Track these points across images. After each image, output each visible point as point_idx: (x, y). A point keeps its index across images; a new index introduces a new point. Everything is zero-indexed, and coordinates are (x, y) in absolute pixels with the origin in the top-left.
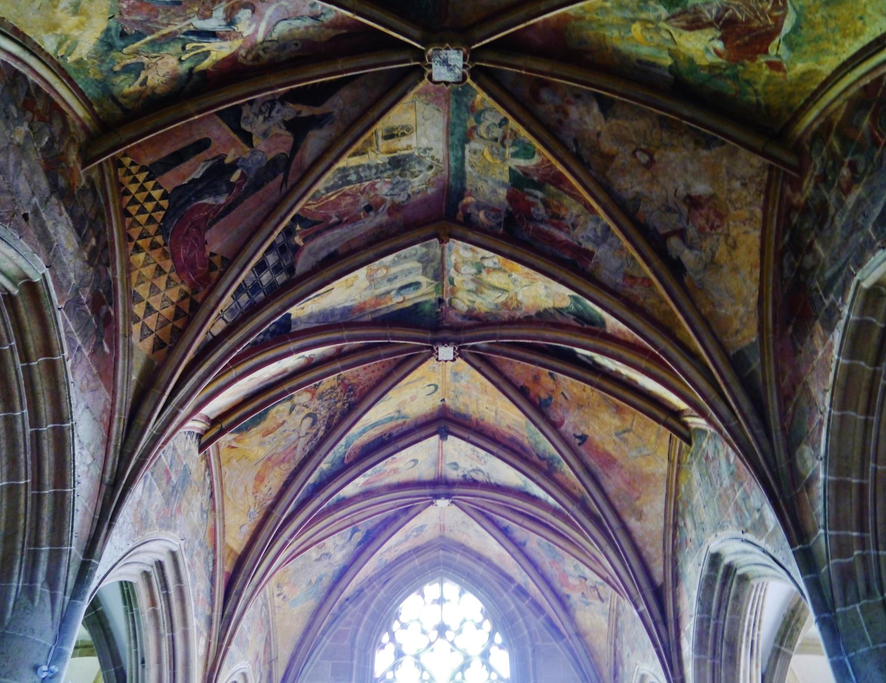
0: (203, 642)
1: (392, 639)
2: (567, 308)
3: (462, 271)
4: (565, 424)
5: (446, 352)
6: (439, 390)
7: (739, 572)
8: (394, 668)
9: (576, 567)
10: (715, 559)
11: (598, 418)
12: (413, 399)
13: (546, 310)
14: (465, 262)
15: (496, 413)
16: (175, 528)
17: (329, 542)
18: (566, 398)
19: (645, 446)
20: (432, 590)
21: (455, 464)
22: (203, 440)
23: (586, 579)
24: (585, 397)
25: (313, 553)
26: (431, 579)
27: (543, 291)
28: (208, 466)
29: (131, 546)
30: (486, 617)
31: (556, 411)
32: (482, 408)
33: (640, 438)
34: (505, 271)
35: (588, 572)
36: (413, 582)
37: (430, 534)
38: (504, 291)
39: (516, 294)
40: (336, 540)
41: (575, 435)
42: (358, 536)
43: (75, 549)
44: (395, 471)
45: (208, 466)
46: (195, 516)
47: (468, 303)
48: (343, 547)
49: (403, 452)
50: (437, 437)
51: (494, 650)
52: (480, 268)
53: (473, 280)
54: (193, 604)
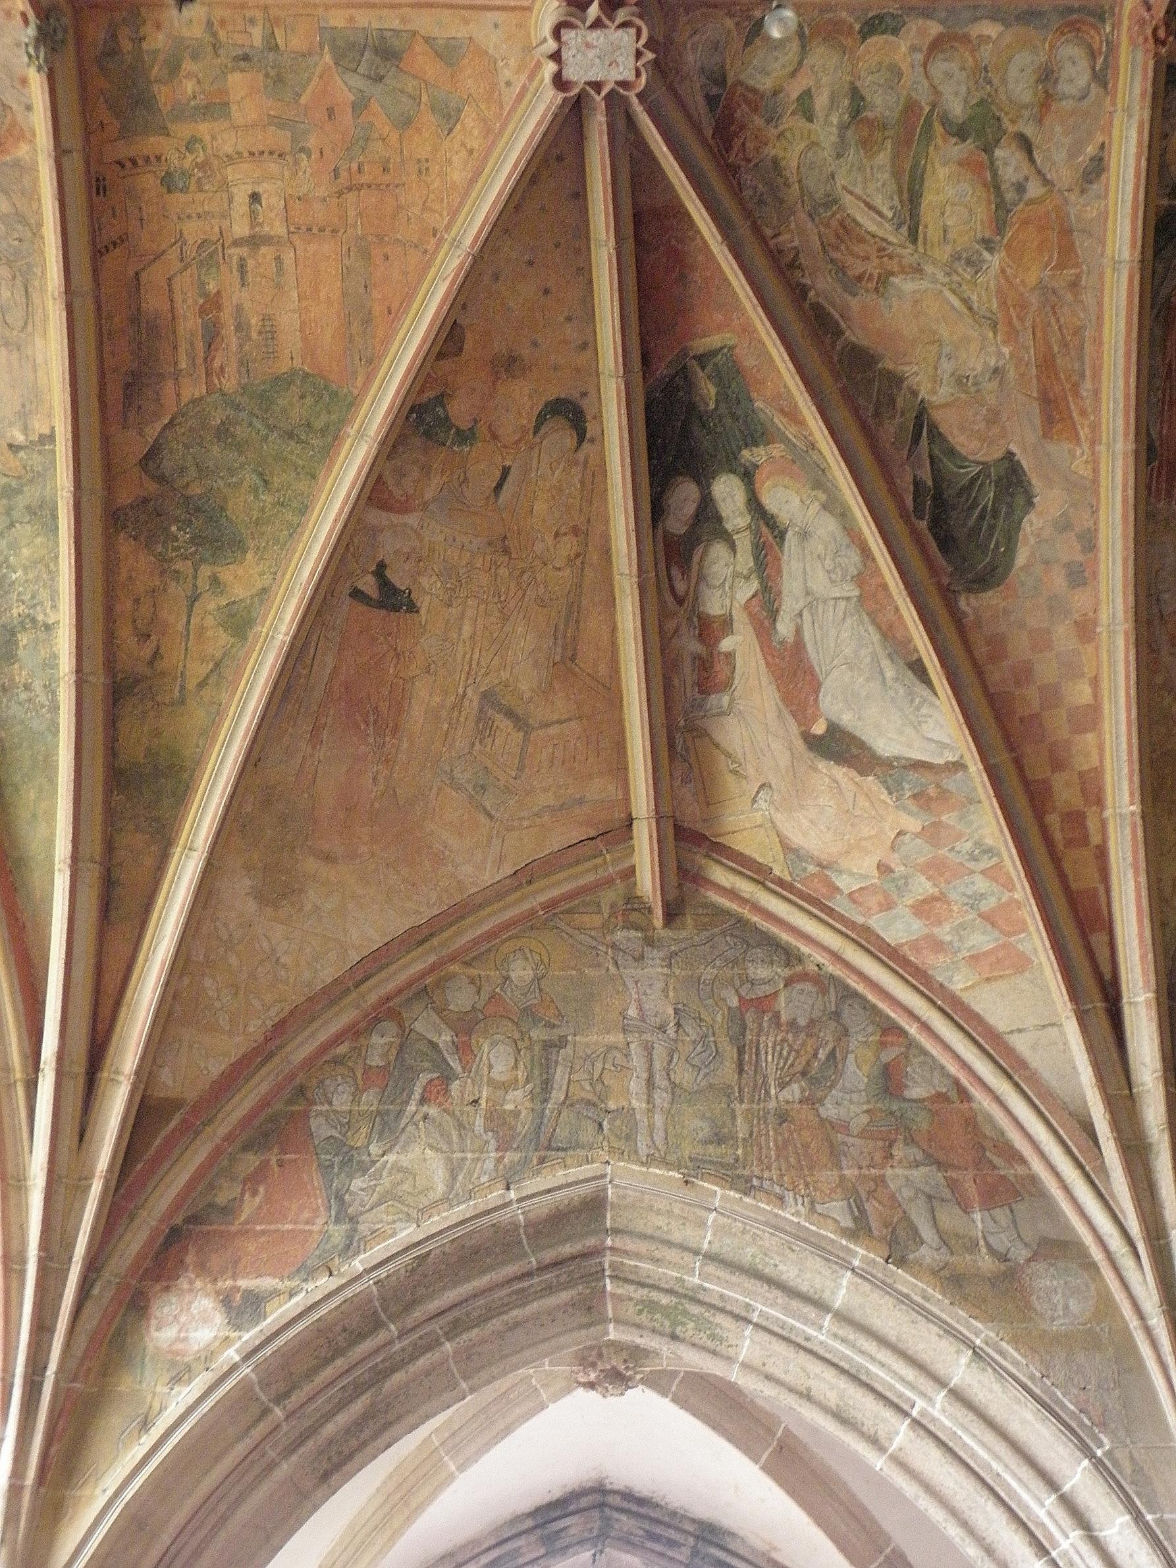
2: (951, 452)
3: (939, 68)
4: (395, 518)
11: (505, 618)
13: (896, 380)
14: (981, 74)
15: (254, 242)
18: (499, 487)
19: (507, 790)
24: (539, 548)
27: (976, 362)
31: (426, 470)
32: (241, 181)
33: (521, 768)
34: (1000, 226)
39: (918, 270)
41: (382, 566)
47: (794, 91)
52: (981, 129)
53: (911, 107)
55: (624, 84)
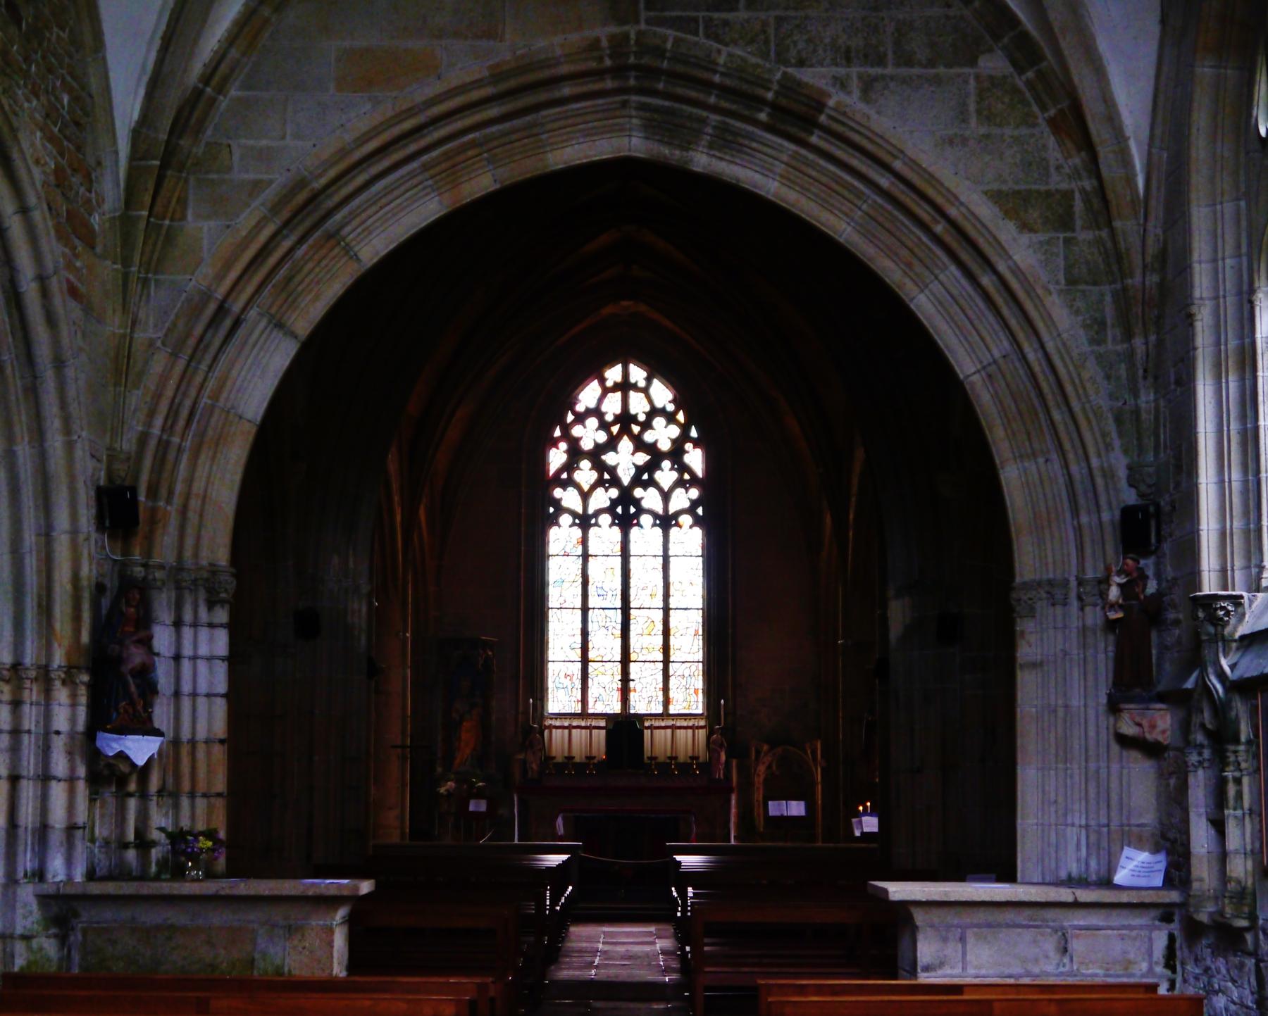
1: (566, 436)
8: (570, 466)
20: (614, 374)
51: (688, 446)
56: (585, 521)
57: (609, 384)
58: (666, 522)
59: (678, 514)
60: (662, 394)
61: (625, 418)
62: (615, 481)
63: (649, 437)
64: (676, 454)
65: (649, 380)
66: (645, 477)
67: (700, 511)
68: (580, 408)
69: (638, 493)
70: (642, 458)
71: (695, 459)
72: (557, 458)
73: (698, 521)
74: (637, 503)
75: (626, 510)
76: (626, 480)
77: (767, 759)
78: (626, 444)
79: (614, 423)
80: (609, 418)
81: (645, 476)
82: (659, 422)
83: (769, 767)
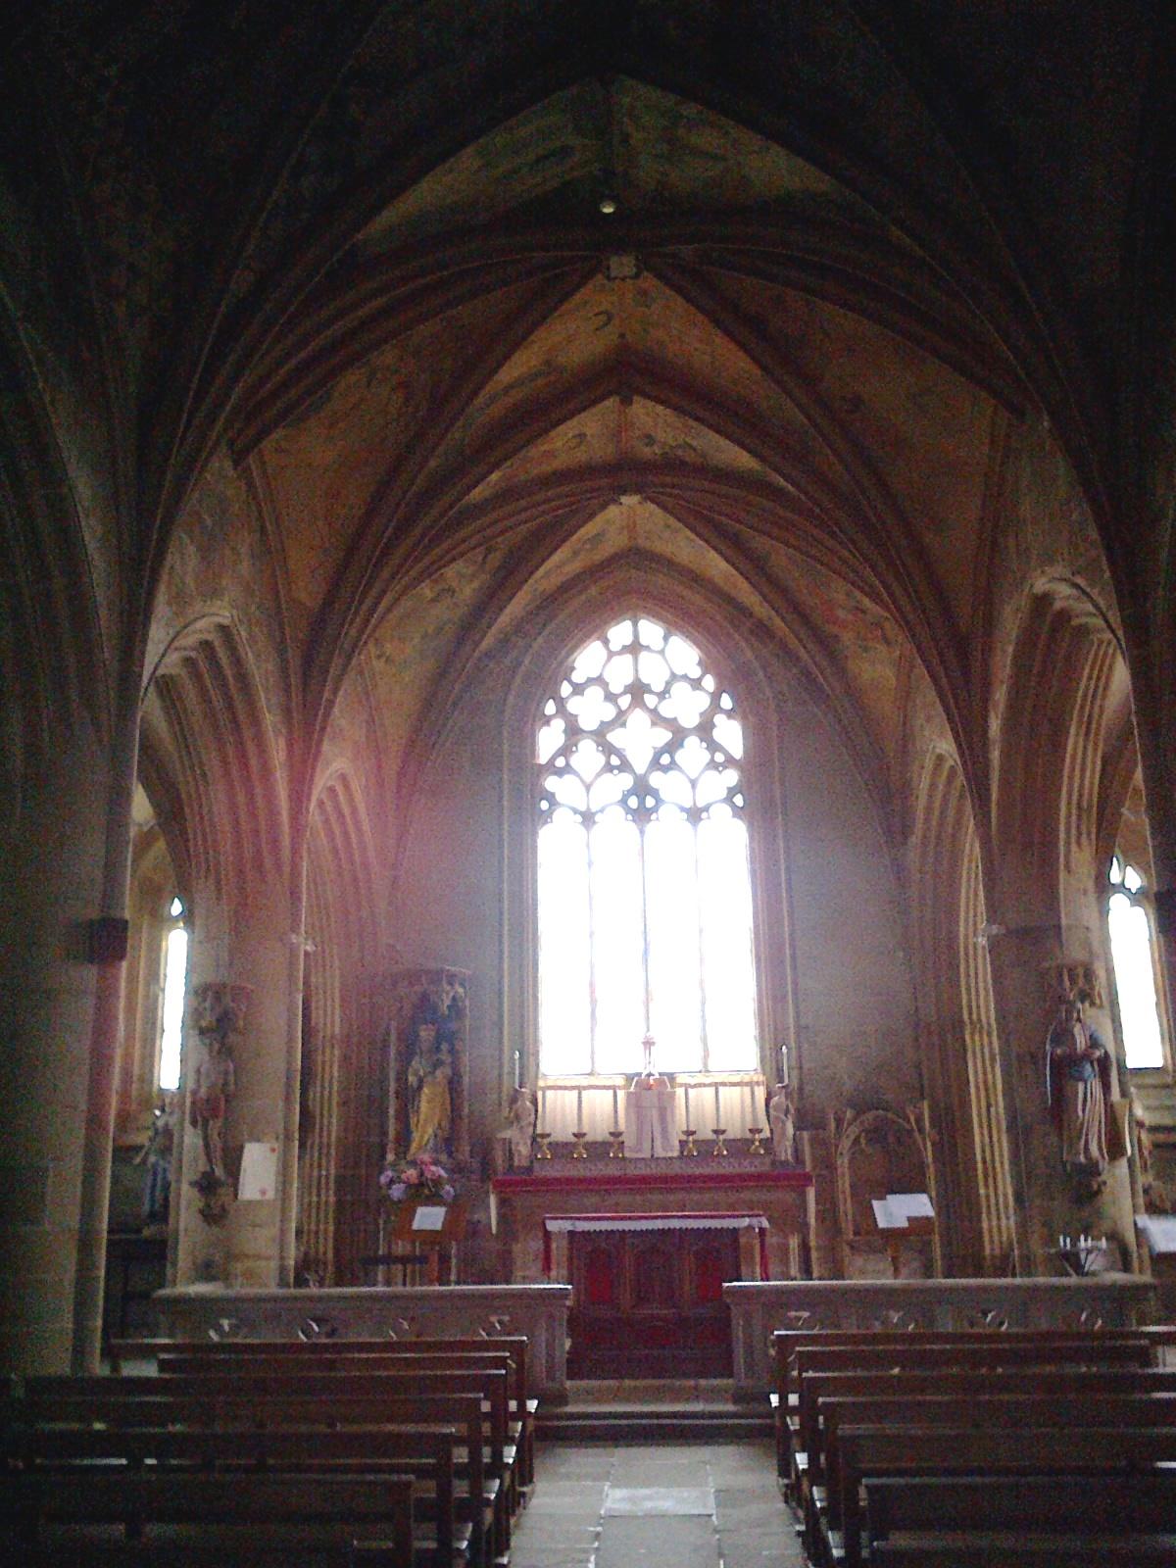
0: (282, 743)
1: (561, 710)
5: (622, 265)
6: (616, 321)
7: (1075, 622)
8: (566, 751)
9: (848, 594)
10: (1043, 601)
12: (570, 340)
16: (223, 594)
17: (450, 572)
20: (620, 633)
21: (649, 436)
22: (239, 445)
23: (863, 612)
25: (426, 590)
26: (615, 617)
28: (250, 485)
29: (172, 632)
30: (705, 673)
35: (867, 602)
36: (591, 621)
37: (615, 542)
38: (715, 158)
40: (459, 566)
42: (495, 559)
43: (108, 655)
44: (551, 454)
45: (250, 485)
46: (245, 567)
48: (473, 576)
49: (561, 428)
50: (611, 403)
51: (720, 719)
54: (262, 694)
55: (637, 258)
56: (588, 818)
57: (615, 646)
58: (695, 814)
59: (706, 809)
60: (686, 654)
61: (637, 690)
62: (625, 766)
63: (667, 709)
64: (705, 729)
65: (666, 639)
66: (665, 759)
67: (739, 800)
68: (578, 677)
69: (656, 779)
70: (664, 736)
71: (731, 734)
72: (549, 740)
73: (738, 812)
74: (655, 793)
75: (642, 802)
76: (640, 765)
77: (853, 1131)
78: (638, 719)
79: (624, 693)
80: (616, 688)
81: (664, 758)
82: (681, 689)
83: (856, 1141)
